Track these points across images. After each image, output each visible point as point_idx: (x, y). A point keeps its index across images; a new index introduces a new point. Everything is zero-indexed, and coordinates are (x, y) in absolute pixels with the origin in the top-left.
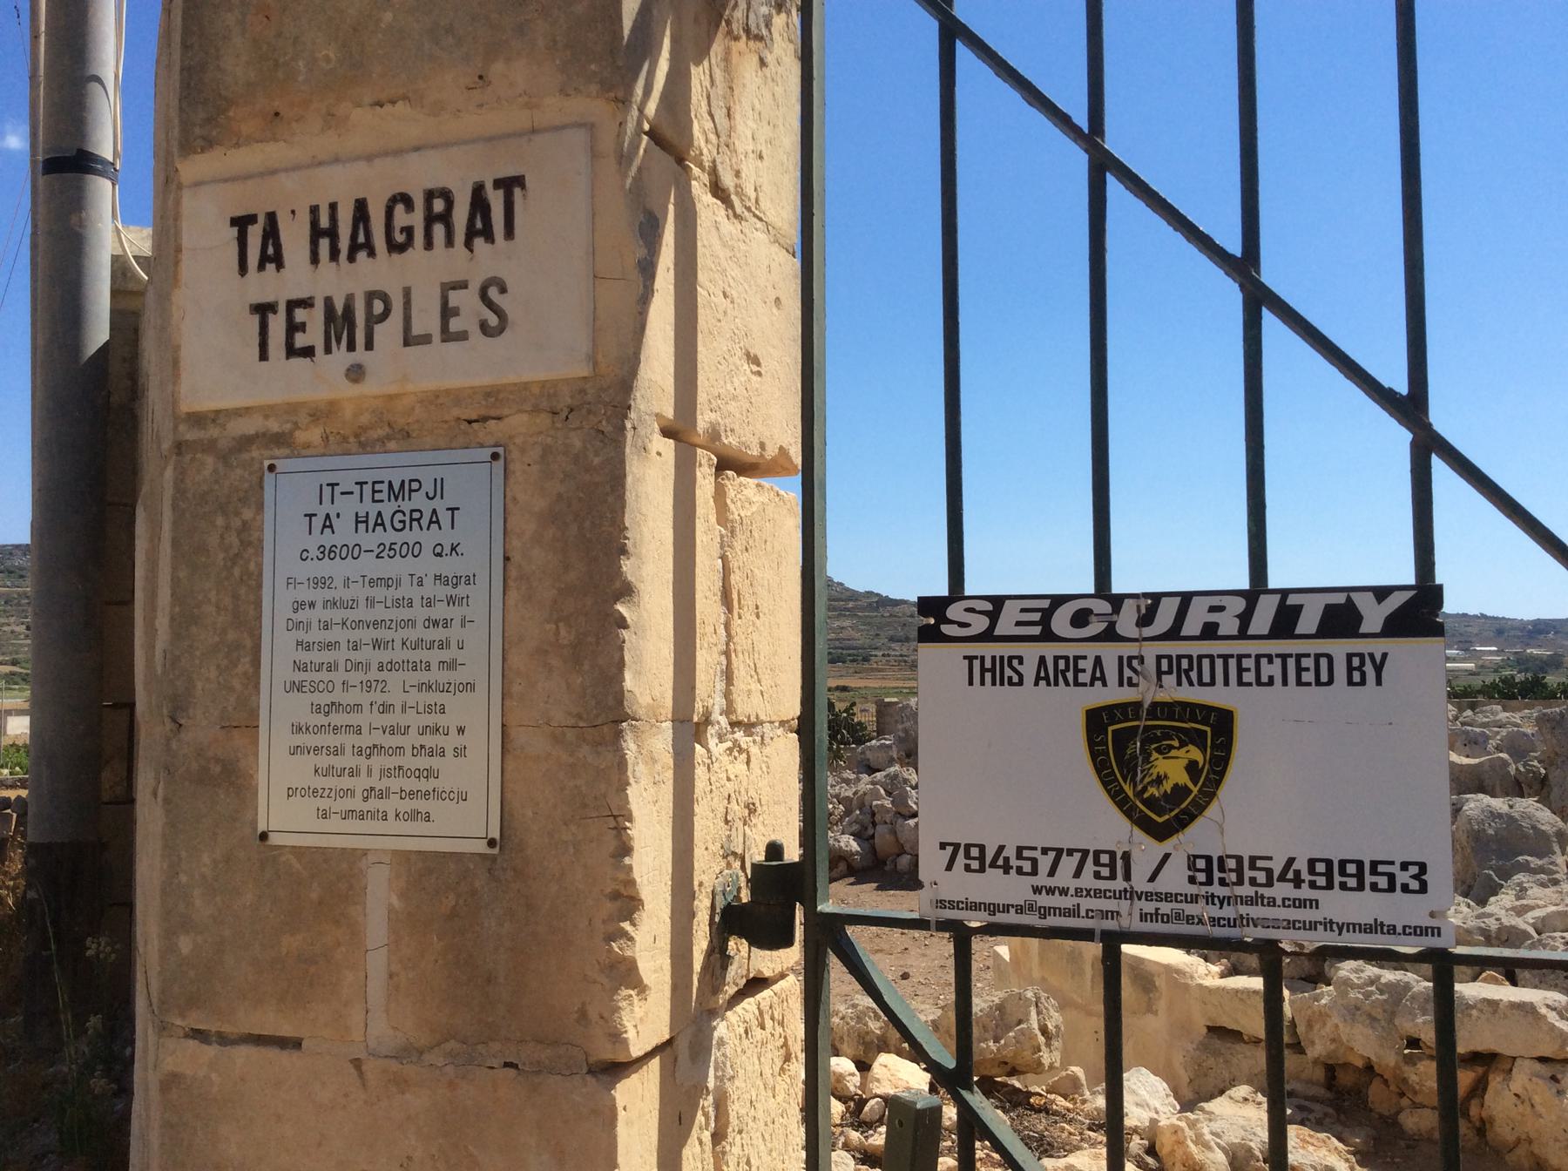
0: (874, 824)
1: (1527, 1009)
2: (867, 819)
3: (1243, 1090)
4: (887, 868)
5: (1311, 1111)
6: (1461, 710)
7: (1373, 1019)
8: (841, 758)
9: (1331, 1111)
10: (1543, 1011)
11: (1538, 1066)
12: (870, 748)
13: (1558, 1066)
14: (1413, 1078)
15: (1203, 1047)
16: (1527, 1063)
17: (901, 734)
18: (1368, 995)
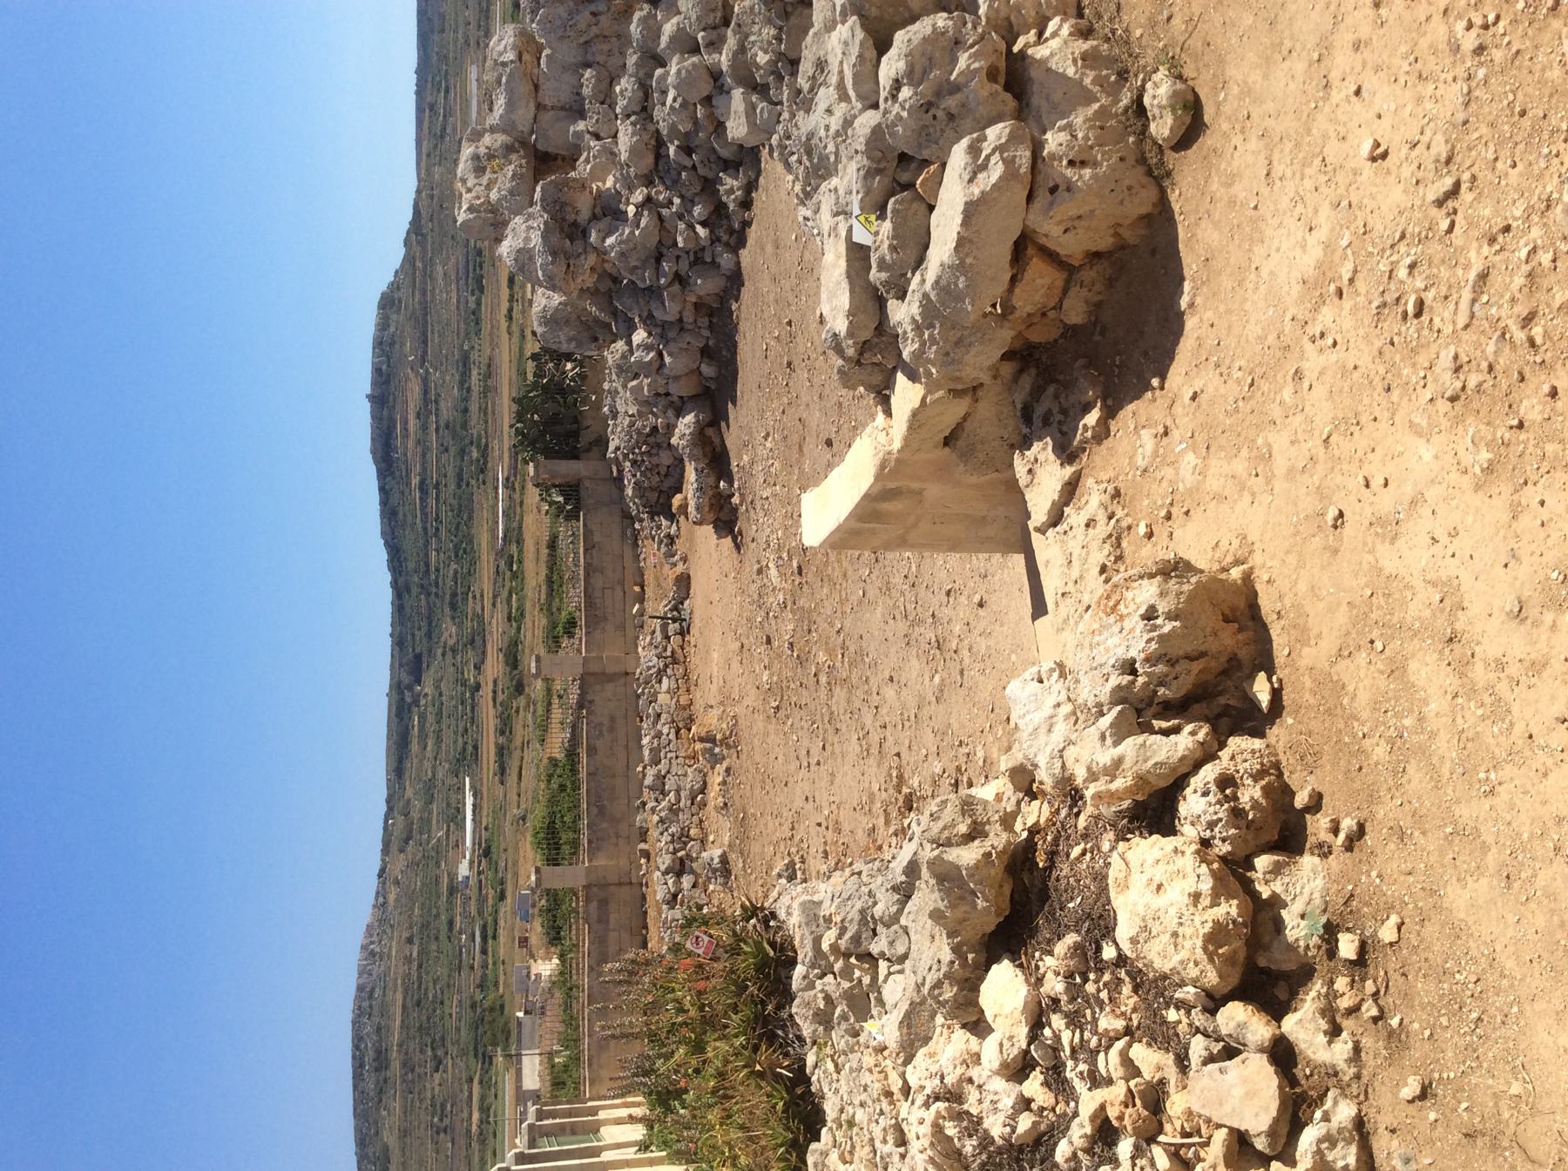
0: (667, 394)
1: (971, 211)
2: (662, 401)
3: (1020, 466)
5: (1049, 413)
7: (957, 343)
9: (1051, 389)
10: (976, 191)
11: (1038, 204)
13: (1040, 178)
14: (1029, 309)
15: (966, 456)
16: (1031, 217)
17: (573, 344)
18: (933, 341)
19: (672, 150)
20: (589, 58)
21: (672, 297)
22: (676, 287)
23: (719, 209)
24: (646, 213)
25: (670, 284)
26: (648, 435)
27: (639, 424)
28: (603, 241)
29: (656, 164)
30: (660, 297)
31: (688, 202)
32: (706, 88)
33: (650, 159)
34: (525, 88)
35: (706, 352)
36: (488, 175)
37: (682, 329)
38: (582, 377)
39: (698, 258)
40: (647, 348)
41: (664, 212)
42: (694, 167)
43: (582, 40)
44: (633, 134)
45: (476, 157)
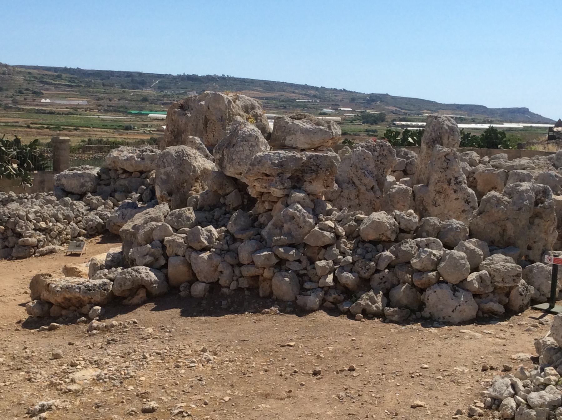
4: (182, 294)
6: (482, 156)
8: (28, 181)
12: (65, 176)
17: (164, 177)
19: (387, 253)
20: (345, 185)
21: (267, 258)
22: (274, 261)
23: (349, 294)
25: (276, 256)
26: (13, 230)
27: (22, 222)
28: (299, 203)
29: (370, 242)
30: (260, 249)
31: (351, 267)
32: (453, 279)
33: (372, 236)
34: (317, 141)
35: (214, 286)
36: (245, 115)
37: (232, 266)
38: (9, 176)
39: (303, 281)
40: (210, 238)
42: (377, 271)
43: (355, 180)
44: (390, 224)
45: (253, 107)
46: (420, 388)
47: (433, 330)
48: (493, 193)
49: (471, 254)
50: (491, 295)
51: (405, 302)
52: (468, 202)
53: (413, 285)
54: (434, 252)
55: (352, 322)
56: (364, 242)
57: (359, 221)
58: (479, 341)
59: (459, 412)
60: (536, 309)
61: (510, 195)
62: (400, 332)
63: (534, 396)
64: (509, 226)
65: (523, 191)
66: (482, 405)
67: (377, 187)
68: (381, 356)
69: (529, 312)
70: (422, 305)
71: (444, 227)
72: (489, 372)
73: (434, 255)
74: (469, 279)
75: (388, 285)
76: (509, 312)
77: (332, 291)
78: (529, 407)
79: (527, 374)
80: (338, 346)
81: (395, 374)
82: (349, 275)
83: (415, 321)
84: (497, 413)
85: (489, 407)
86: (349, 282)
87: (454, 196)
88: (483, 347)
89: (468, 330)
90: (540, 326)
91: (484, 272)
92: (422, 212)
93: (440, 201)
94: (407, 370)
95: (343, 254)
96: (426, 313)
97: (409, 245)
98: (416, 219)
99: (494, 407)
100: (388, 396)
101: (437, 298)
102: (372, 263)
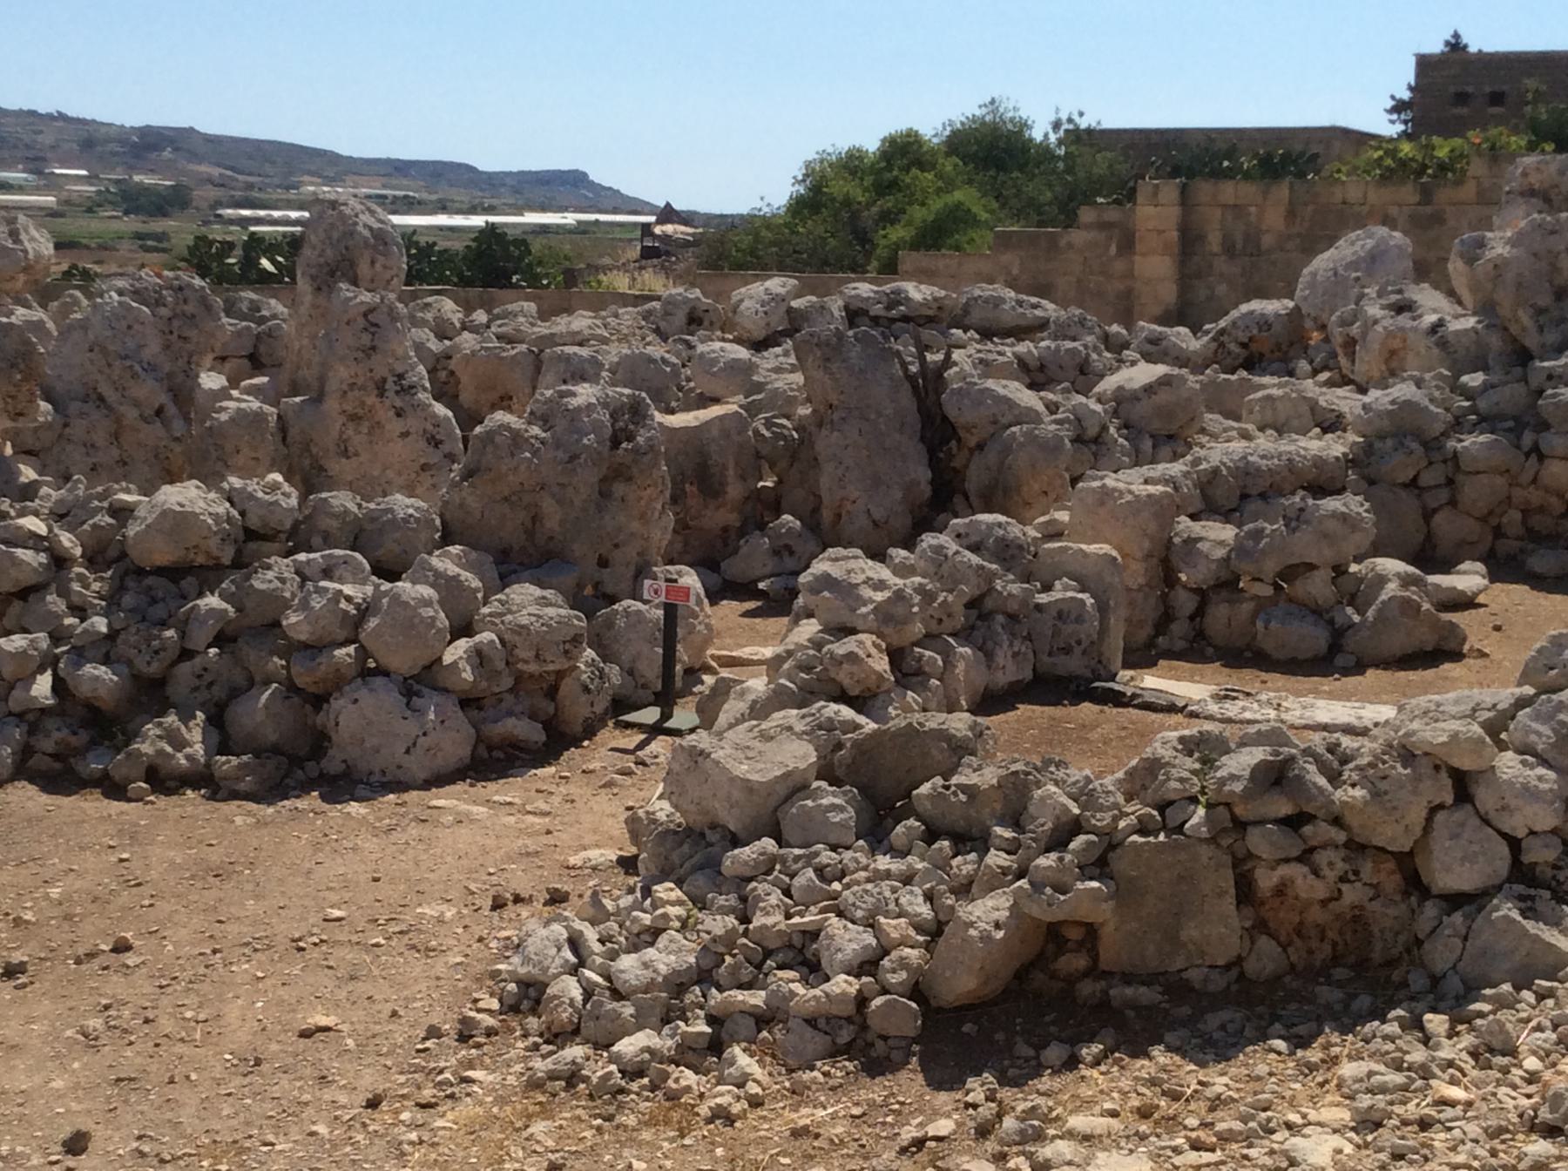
6: (469, 308)
19: (212, 601)
20: (74, 407)
23: (105, 725)
24: (43, 558)
29: (160, 571)
31: (106, 649)
32: (403, 661)
33: (163, 554)
41: (55, 603)
42: (186, 654)
44: (216, 516)
46: (326, 980)
47: (354, 808)
48: (501, 417)
49: (448, 587)
50: (509, 698)
51: (271, 735)
52: (435, 443)
53: (291, 688)
54: (348, 589)
55: (117, 806)
56: (140, 572)
57: (122, 513)
58: (480, 826)
59: (433, 1032)
60: (629, 725)
61: (545, 421)
62: (261, 823)
63: (627, 963)
64: (548, 505)
65: (578, 409)
66: (495, 1004)
67: (172, 410)
68: (210, 896)
69: (611, 737)
70: (320, 742)
71: (372, 517)
72: (511, 911)
73: (349, 599)
74: (448, 657)
75: (218, 692)
76: (558, 740)
77: (50, 723)
78: (617, 995)
79: (609, 904)
80: (78, 884)
81: (252, 947)
82: (103, 672)
83: (304, 789)
84: (533, 1023)
85: (512, 1008)
86: (102, 692)
87: (396, 426)
88: (490, 842)
89: (447, 799)
90: (639, 770)
91: (486, 636)
92: (309, 479)
93: (357, 440)
94: (286, 928)
95: (81, 611)
96: (333, 763)
97: (275, 574)
98: (289, 498)
99: (525, 1005)
100: (232, 1012)
101: (362, 719)
102: (170, 633)
